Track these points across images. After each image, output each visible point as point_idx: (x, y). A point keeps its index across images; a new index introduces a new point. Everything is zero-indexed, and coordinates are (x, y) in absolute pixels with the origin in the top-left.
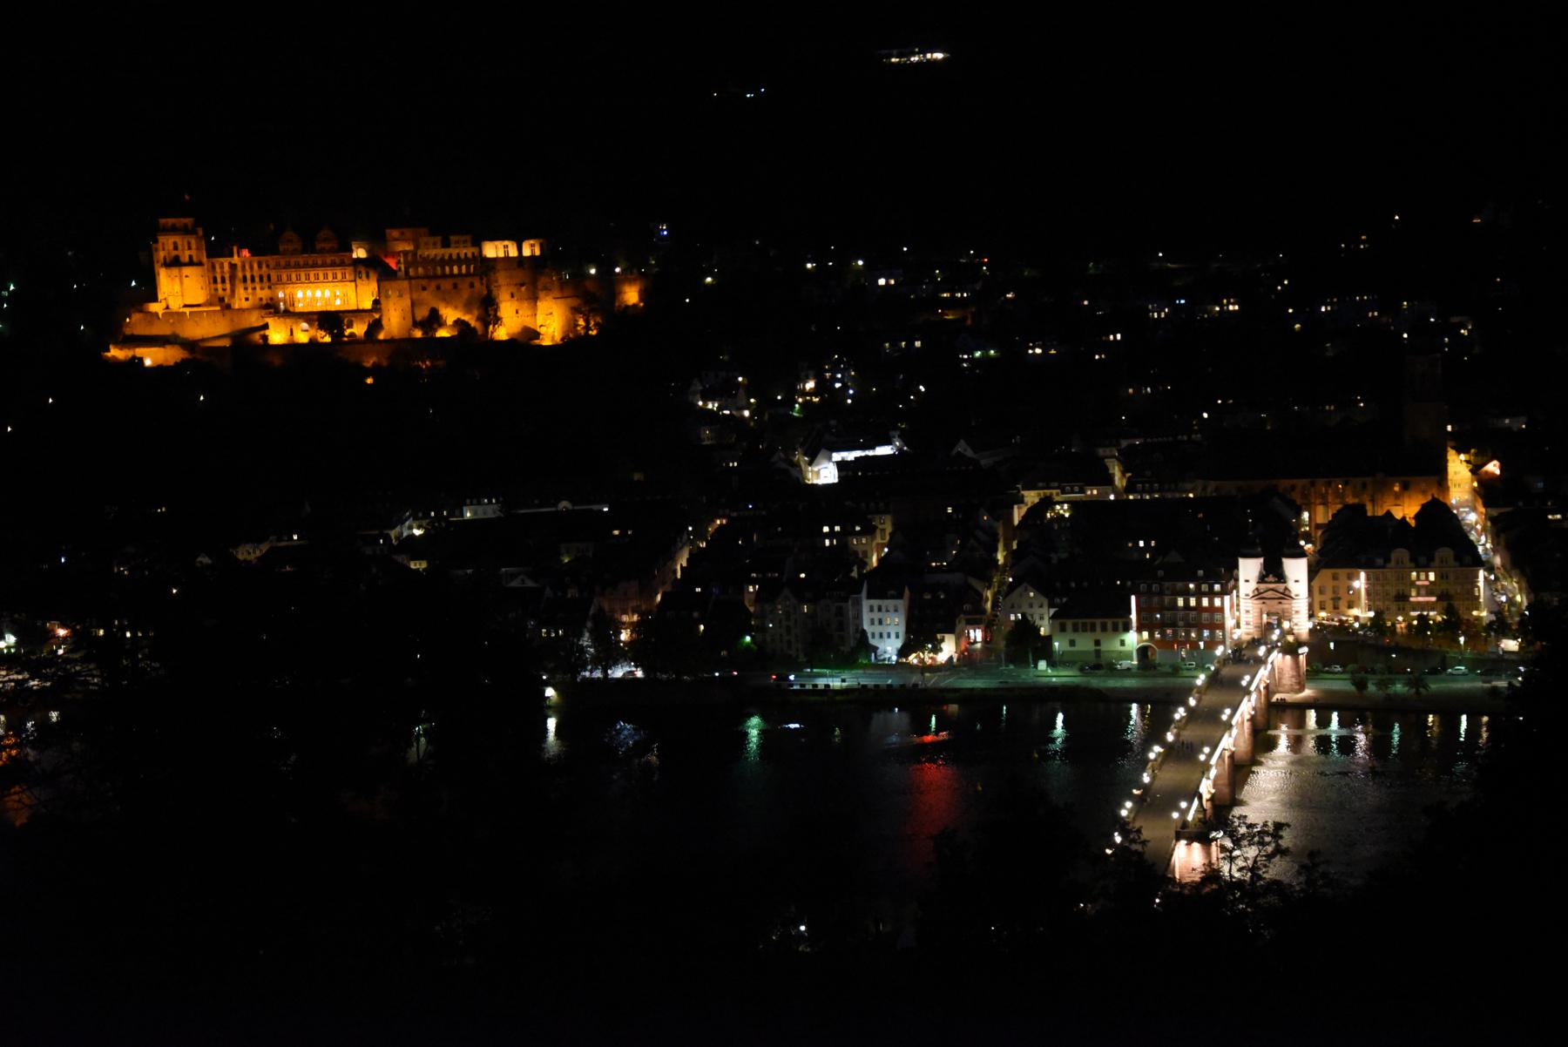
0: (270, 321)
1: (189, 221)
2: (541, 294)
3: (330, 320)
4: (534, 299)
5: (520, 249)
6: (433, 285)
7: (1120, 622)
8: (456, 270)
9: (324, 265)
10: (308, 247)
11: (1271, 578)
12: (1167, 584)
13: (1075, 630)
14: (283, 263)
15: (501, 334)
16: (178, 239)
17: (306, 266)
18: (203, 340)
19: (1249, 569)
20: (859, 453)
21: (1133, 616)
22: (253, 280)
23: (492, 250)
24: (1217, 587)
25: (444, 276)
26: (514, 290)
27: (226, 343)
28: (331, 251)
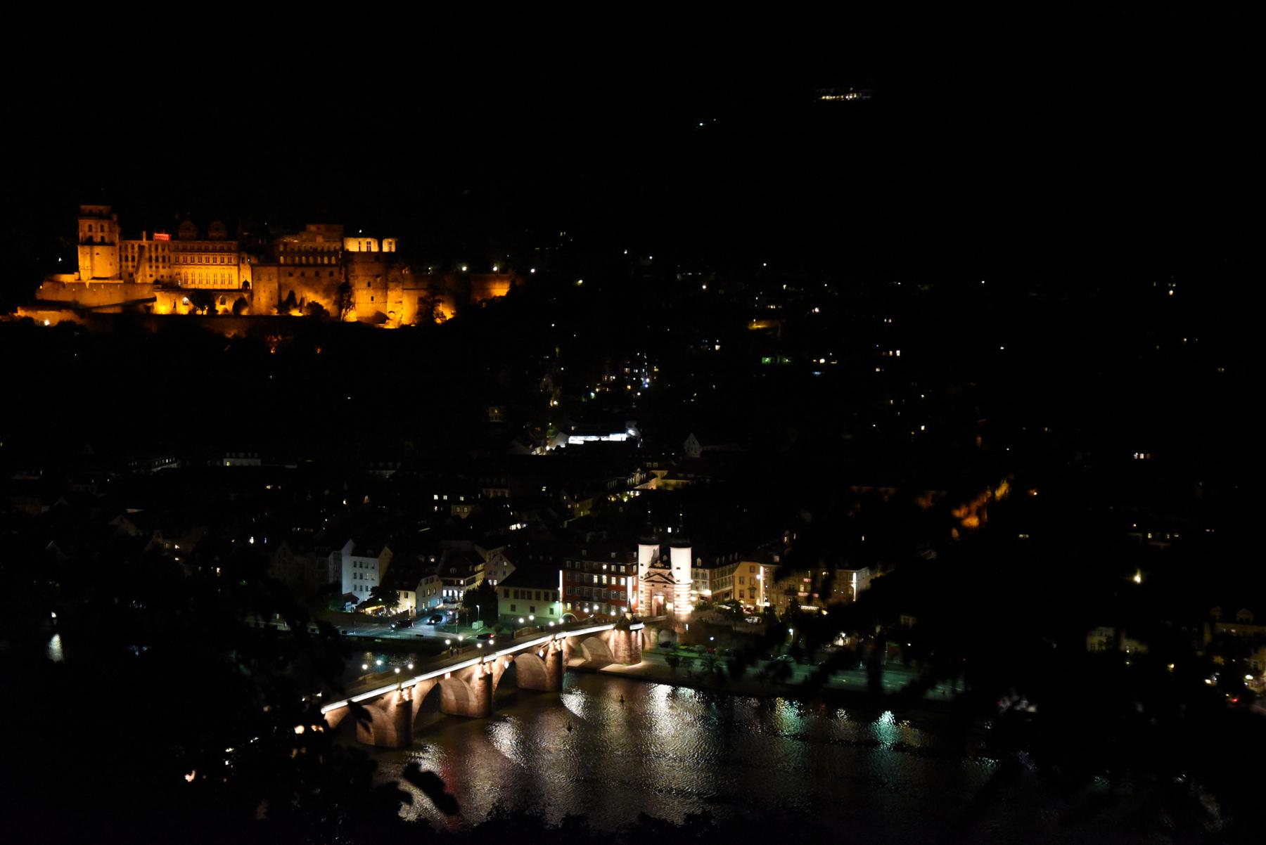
0: (157, 294)
1: (103, 208)
2: (391, 285)
3: (203, 297)
4: (385, 288)
5: (380, 246)
6: (298, 273)
7: (550, 592)
8: (326, 261)
9: (214, 251)
10: (203, 235)
11: (658, 564)
12: (586, 563)
13: (516, 597)
14: (180, 247)
15: (352, 316)
16: (92, 222)
17: (199, 250)
18: (99, 307)
19: (646, 553)
20: (604, 439)
21: (561, 589)
22: (157, 260)
23: (353, 246)
24: (623, 569)
25: (308, 265)
26: (371, 280)
27: (117, 310)
28: (220, 239)
